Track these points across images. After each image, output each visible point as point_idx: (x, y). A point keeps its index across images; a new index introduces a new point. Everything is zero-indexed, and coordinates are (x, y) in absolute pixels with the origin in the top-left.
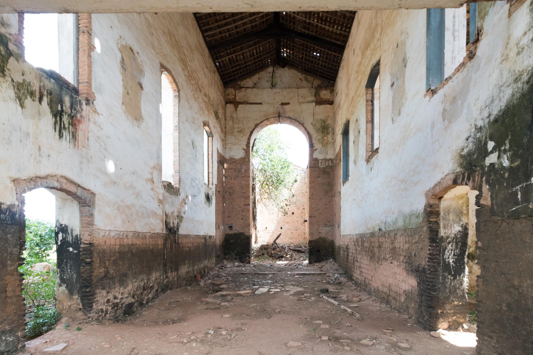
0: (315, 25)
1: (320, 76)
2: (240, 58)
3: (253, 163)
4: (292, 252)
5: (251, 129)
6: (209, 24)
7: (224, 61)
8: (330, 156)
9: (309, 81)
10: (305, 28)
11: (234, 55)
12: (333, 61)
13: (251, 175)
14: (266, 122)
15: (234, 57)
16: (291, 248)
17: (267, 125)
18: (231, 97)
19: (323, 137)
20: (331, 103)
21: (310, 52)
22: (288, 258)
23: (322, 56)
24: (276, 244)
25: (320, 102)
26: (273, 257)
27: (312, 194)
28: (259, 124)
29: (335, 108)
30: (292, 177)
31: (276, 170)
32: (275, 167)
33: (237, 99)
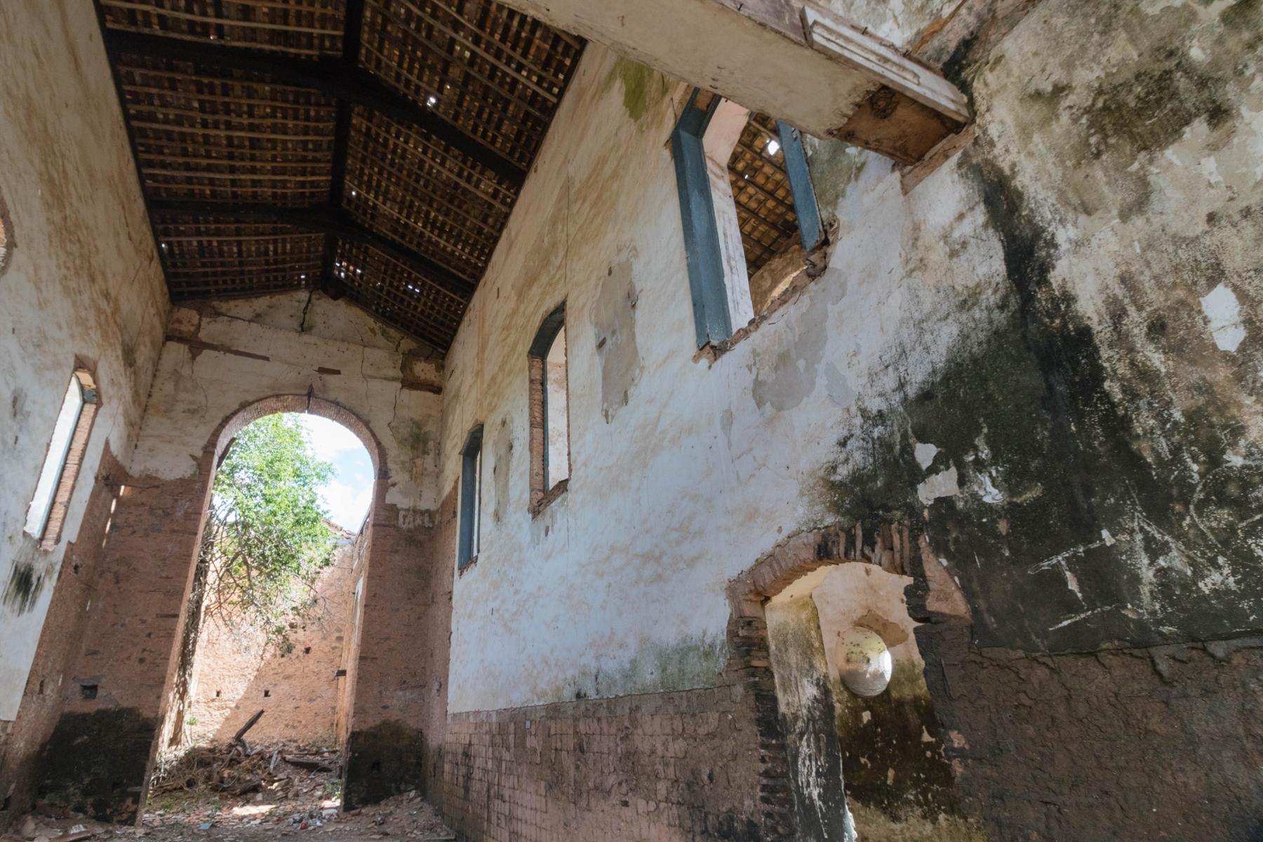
0: (418, 231)
1: (415, 333)
2: (231, 250)
3: (217, 501)
4: (290, 769)
6: (162, 153)
7: (185, 244)
8: (428, 502)
10: (395, 232)
11: (215, 241)
12: (448, 310)
13: (201, 533)
14: (272, 403)
15: (215, 244)
16: (289, 757)
17: (274, 411)
18: (186, 328)
19: (412, 459)
20: (438, 390)
21: (400, 281)
22: (274, 792)
23: (425, 293)
24: (243, 745)
25: (411, 383)
26: (224, 790)
27: (375, 596)
28: (251, 403)
29: (446, 402)
30: (322, 550)
31: (279, 527)
32: (279, 518)
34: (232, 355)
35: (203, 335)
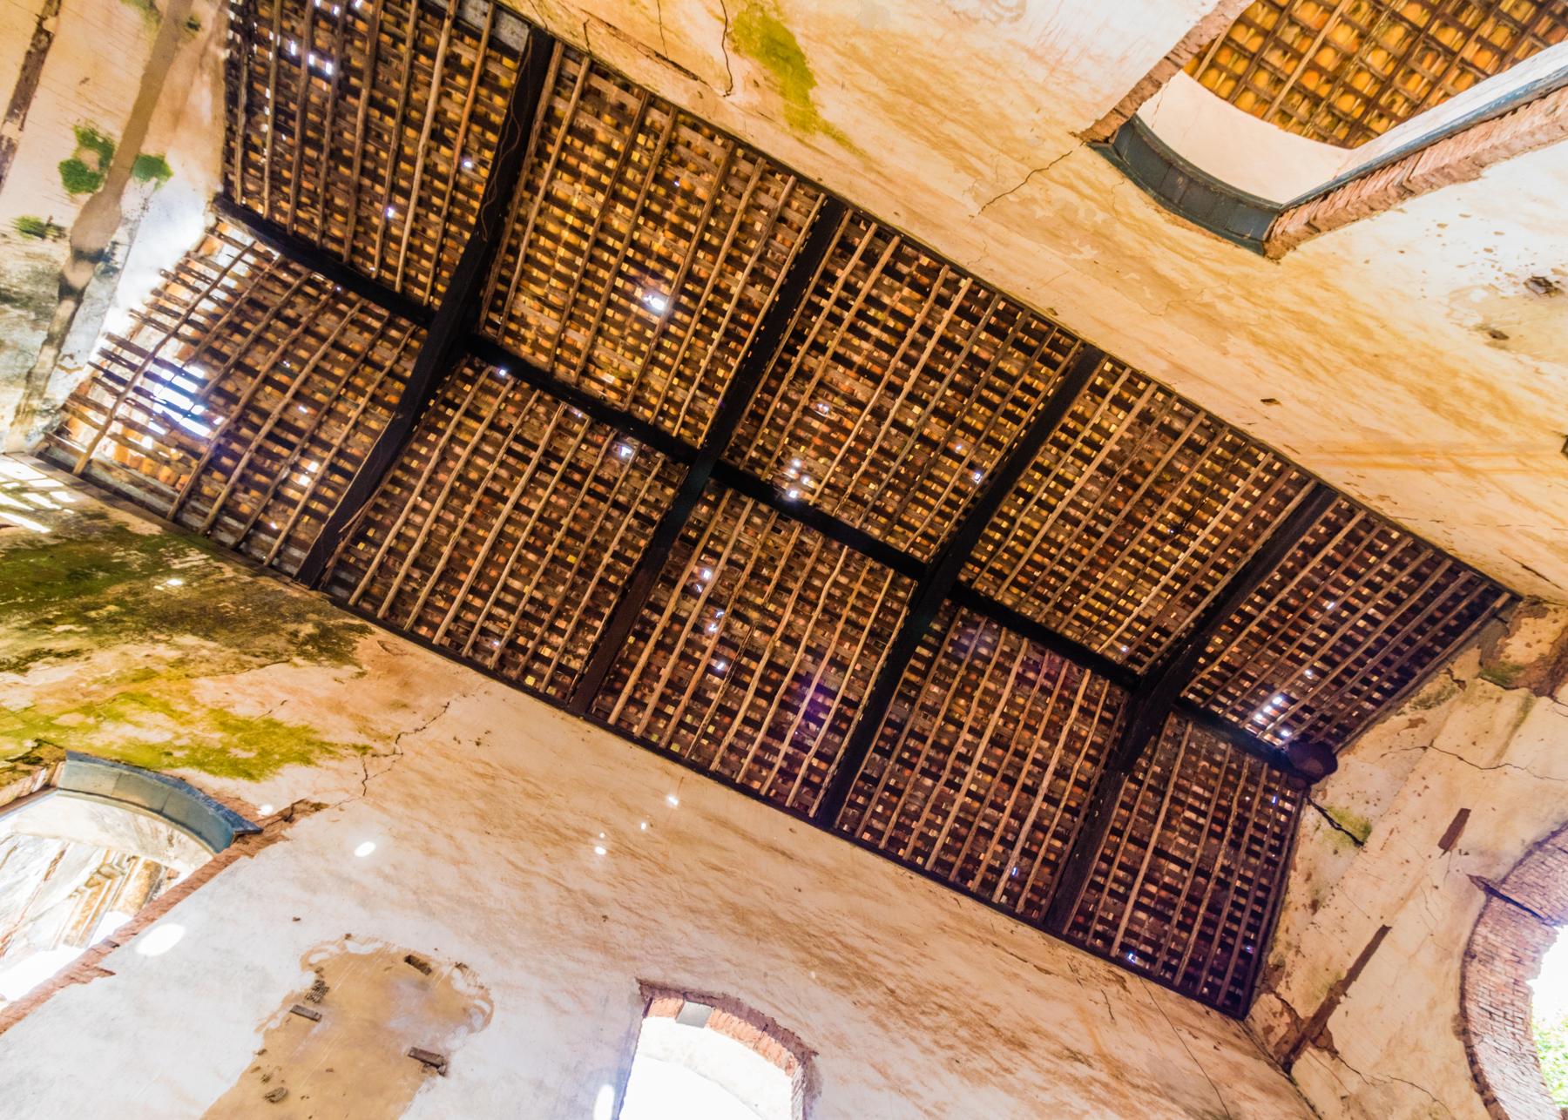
5: (1464, 1069)
9: (1439, 694)
18: (1282, 1027)
28: (1463, 1014)
33: (1301, 1013)
34: (1354, 984)
35: (1306, 1011)
